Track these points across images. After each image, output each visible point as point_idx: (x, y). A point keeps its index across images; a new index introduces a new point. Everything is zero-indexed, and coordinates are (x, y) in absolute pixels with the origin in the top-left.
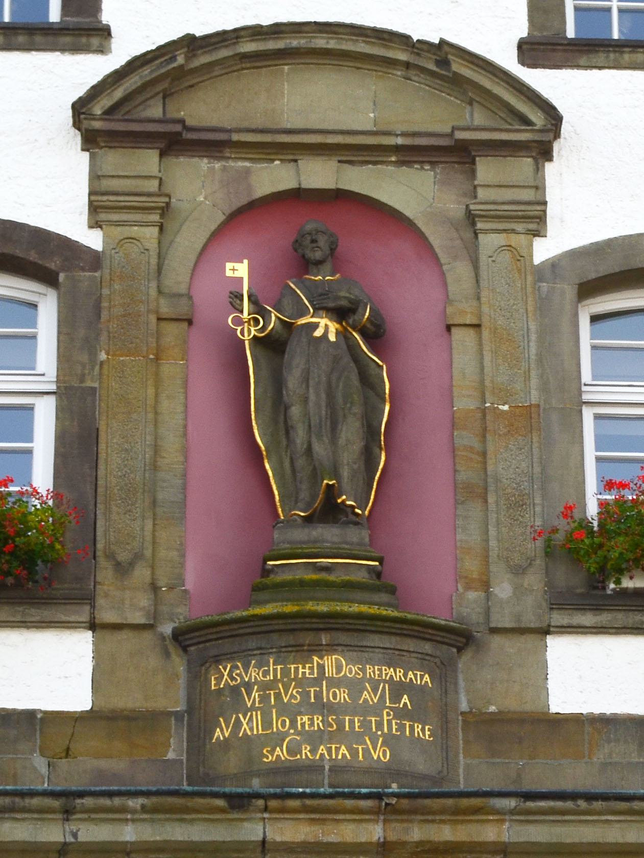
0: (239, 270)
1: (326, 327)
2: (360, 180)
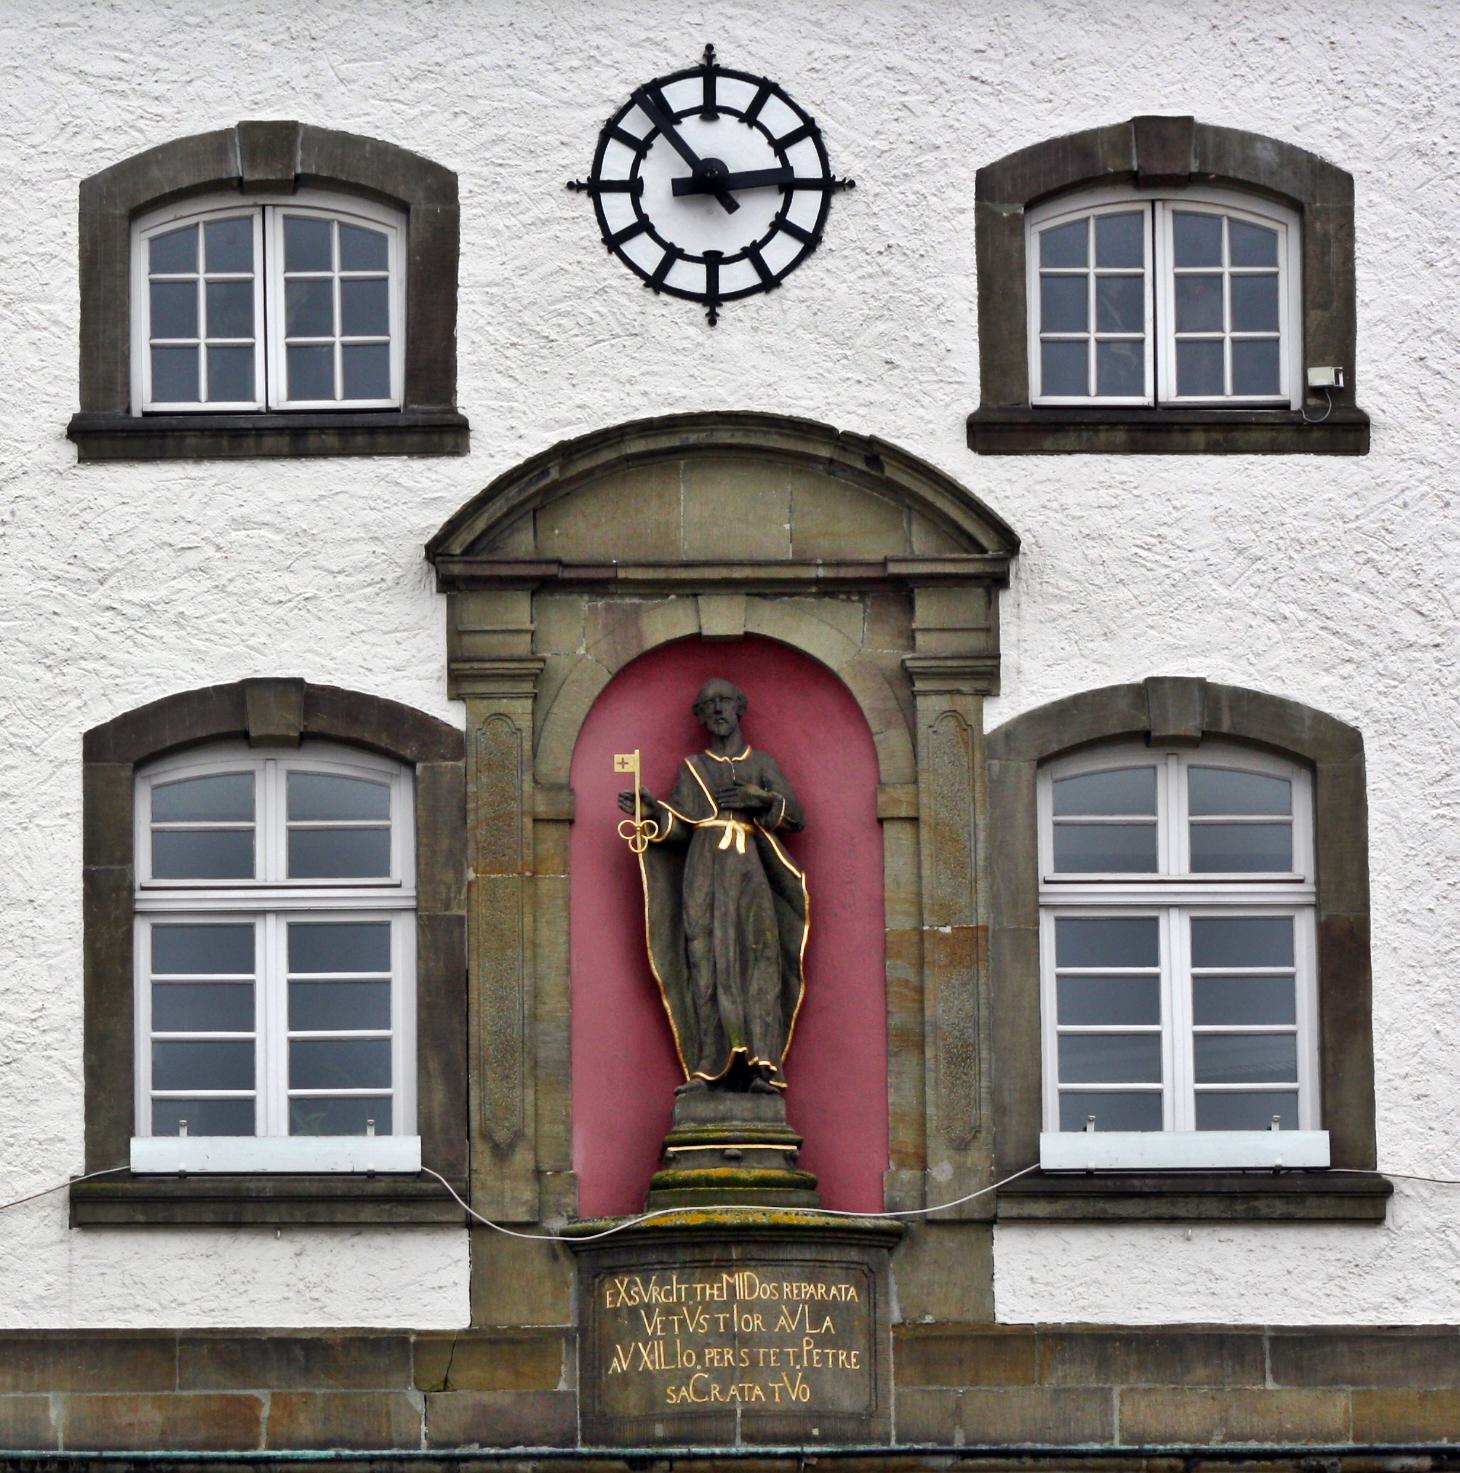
0: (630, 763)
1: (734, 835)
2: (775, 622)
